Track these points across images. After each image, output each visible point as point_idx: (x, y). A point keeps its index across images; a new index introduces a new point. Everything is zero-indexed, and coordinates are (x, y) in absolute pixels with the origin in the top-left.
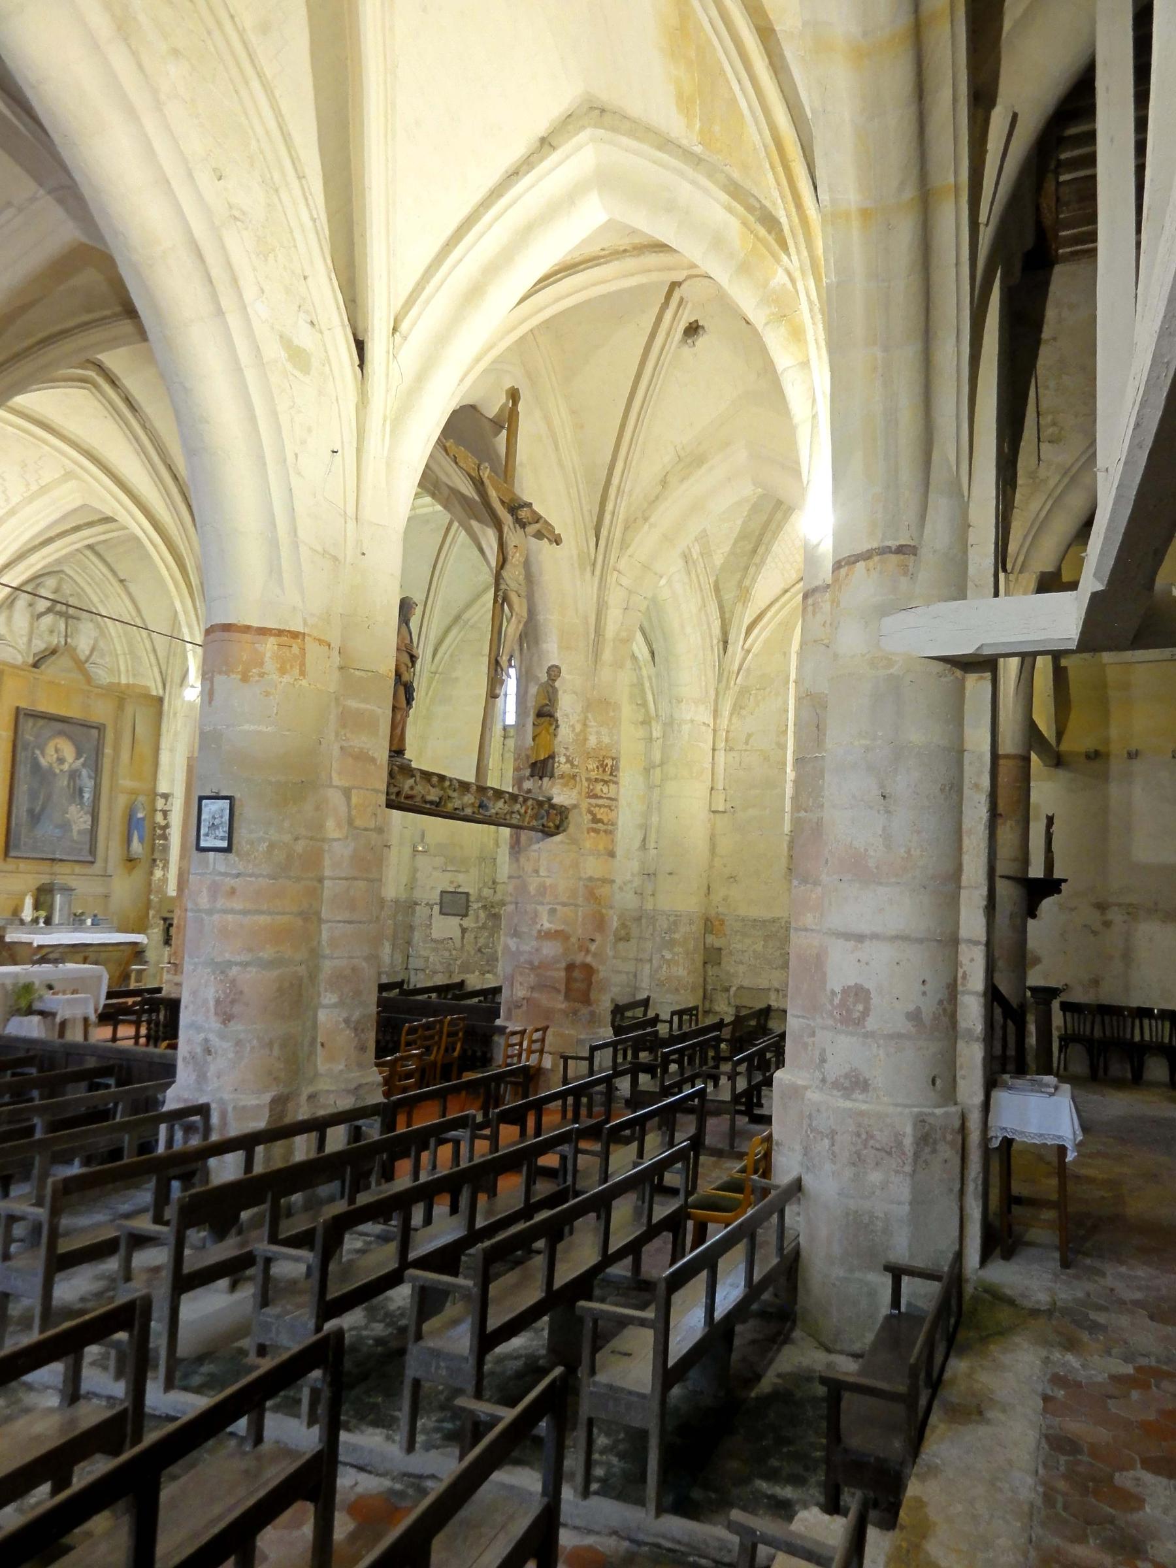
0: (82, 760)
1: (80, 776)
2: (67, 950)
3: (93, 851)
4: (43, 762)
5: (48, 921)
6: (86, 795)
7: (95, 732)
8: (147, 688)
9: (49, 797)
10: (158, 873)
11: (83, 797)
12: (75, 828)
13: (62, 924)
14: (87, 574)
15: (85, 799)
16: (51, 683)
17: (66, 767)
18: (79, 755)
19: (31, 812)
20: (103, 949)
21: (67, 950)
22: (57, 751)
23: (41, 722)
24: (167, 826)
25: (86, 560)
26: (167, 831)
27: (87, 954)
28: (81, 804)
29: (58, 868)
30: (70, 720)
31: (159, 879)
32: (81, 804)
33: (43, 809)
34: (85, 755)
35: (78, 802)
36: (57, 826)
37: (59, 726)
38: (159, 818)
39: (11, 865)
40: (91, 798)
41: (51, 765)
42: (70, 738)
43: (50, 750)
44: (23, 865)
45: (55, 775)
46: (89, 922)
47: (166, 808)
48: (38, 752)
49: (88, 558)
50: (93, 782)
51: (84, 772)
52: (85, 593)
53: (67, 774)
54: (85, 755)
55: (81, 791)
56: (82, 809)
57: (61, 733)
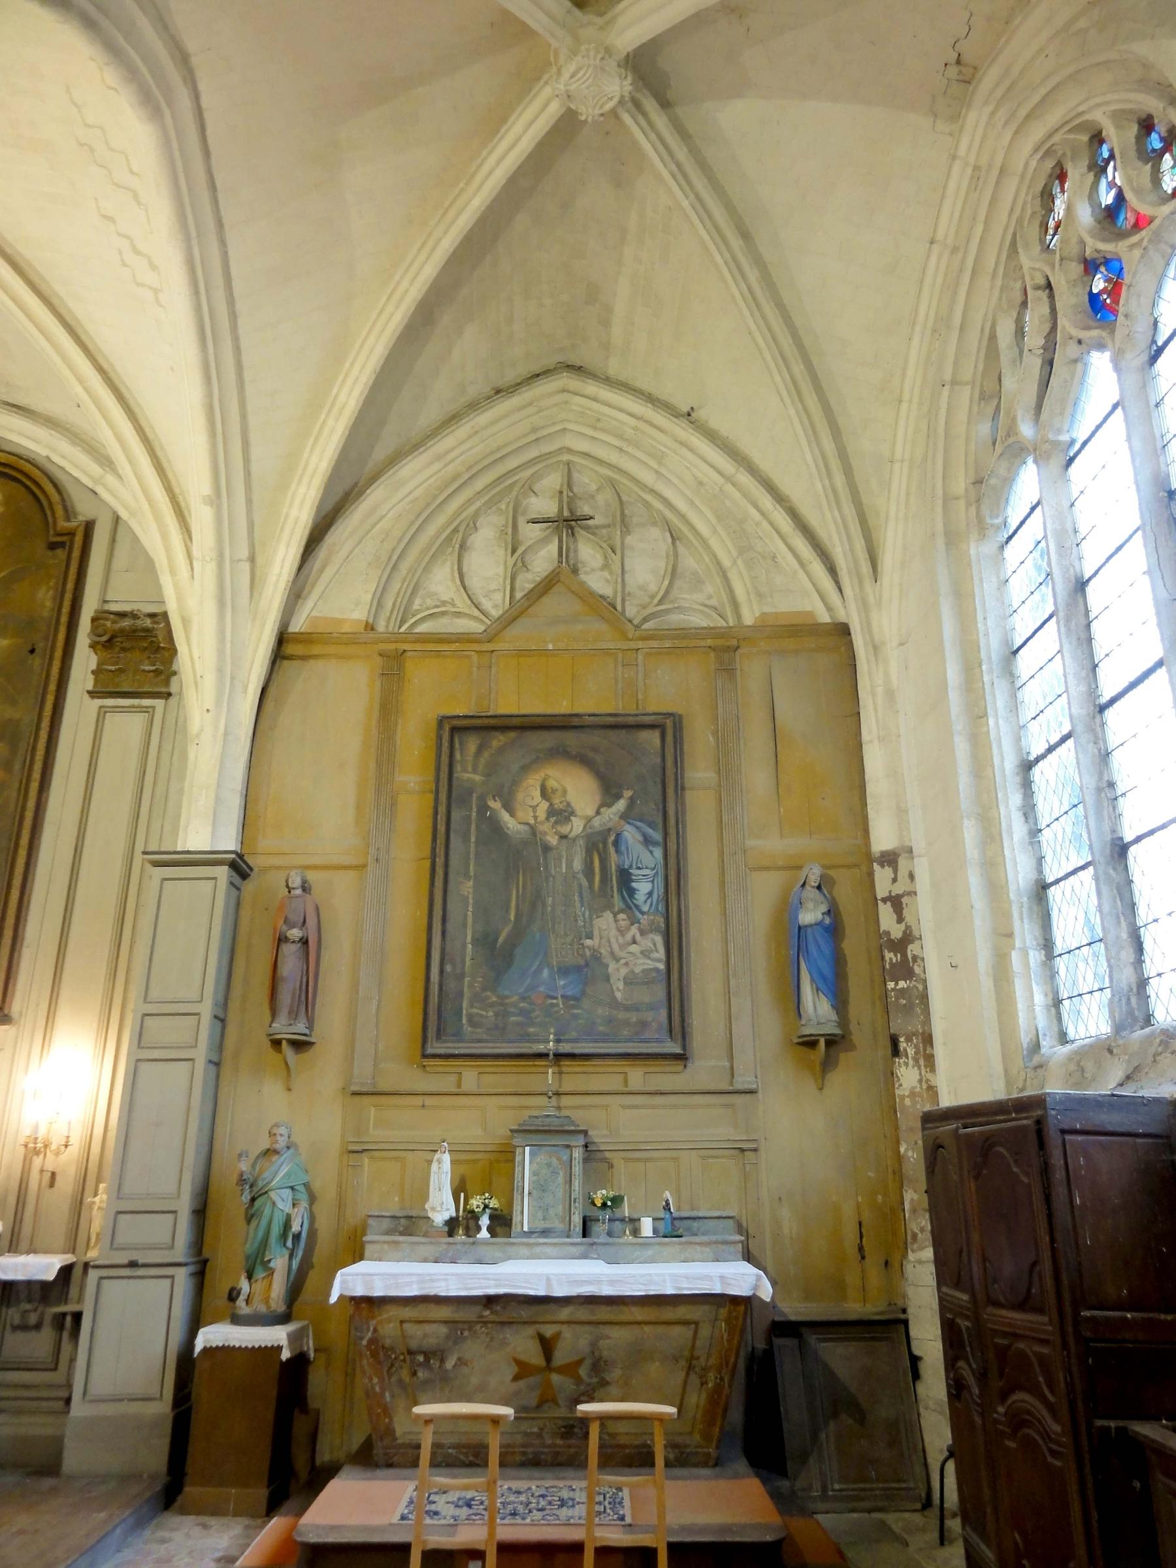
0: (621, 805)
1: (616, 843)
2: (470, 1314)
3: (678, 1026)
4: (510, 823)
5: (501, 1223)
6: (642, 888)
7: (654, 737)
8: (810, 614)
9: (536, 900)
10: (908, 1076)
11: (632, 892)
12: (617, 973)
13: (545, 1233)
14: (603, 430)
15: (640, 897)
16: (521, 653)
17: (577, 826)
18: (610, 791)
19: (486, 941)
20: (603, 1313)
21: (470, 1314)
22: (544, 793)
23: (498, 740)
24: (908, 937)
25: (595, 406)
26: (912, 949)
27: (549, 1331)
28: (630, 907)
29: (576, 1078)
30: (576, 722)
31: (913, 1094)
32: (630, 907)
33: (518, 933)
34: (628, 794)
35: (617, 902)
36: (564, 971)
37: (549, 739)
38: (886, 914)
39: (441, 1079)
40: (660, 890)
41: (533, 830)
42: (583, 760)
43: (530, 793)
44: (470, 1077)
45: (547, 848)
46: (647, 1226)
47: (898, 889)
48: (495, 805)
49: (595, 399)
50: (658, 852)
51: (631, 835)
52: (620, 470)
53: (581, 842)
54: (628, 794)
55: (625, 878)
56: (634, 921)
57: (559, 753)
